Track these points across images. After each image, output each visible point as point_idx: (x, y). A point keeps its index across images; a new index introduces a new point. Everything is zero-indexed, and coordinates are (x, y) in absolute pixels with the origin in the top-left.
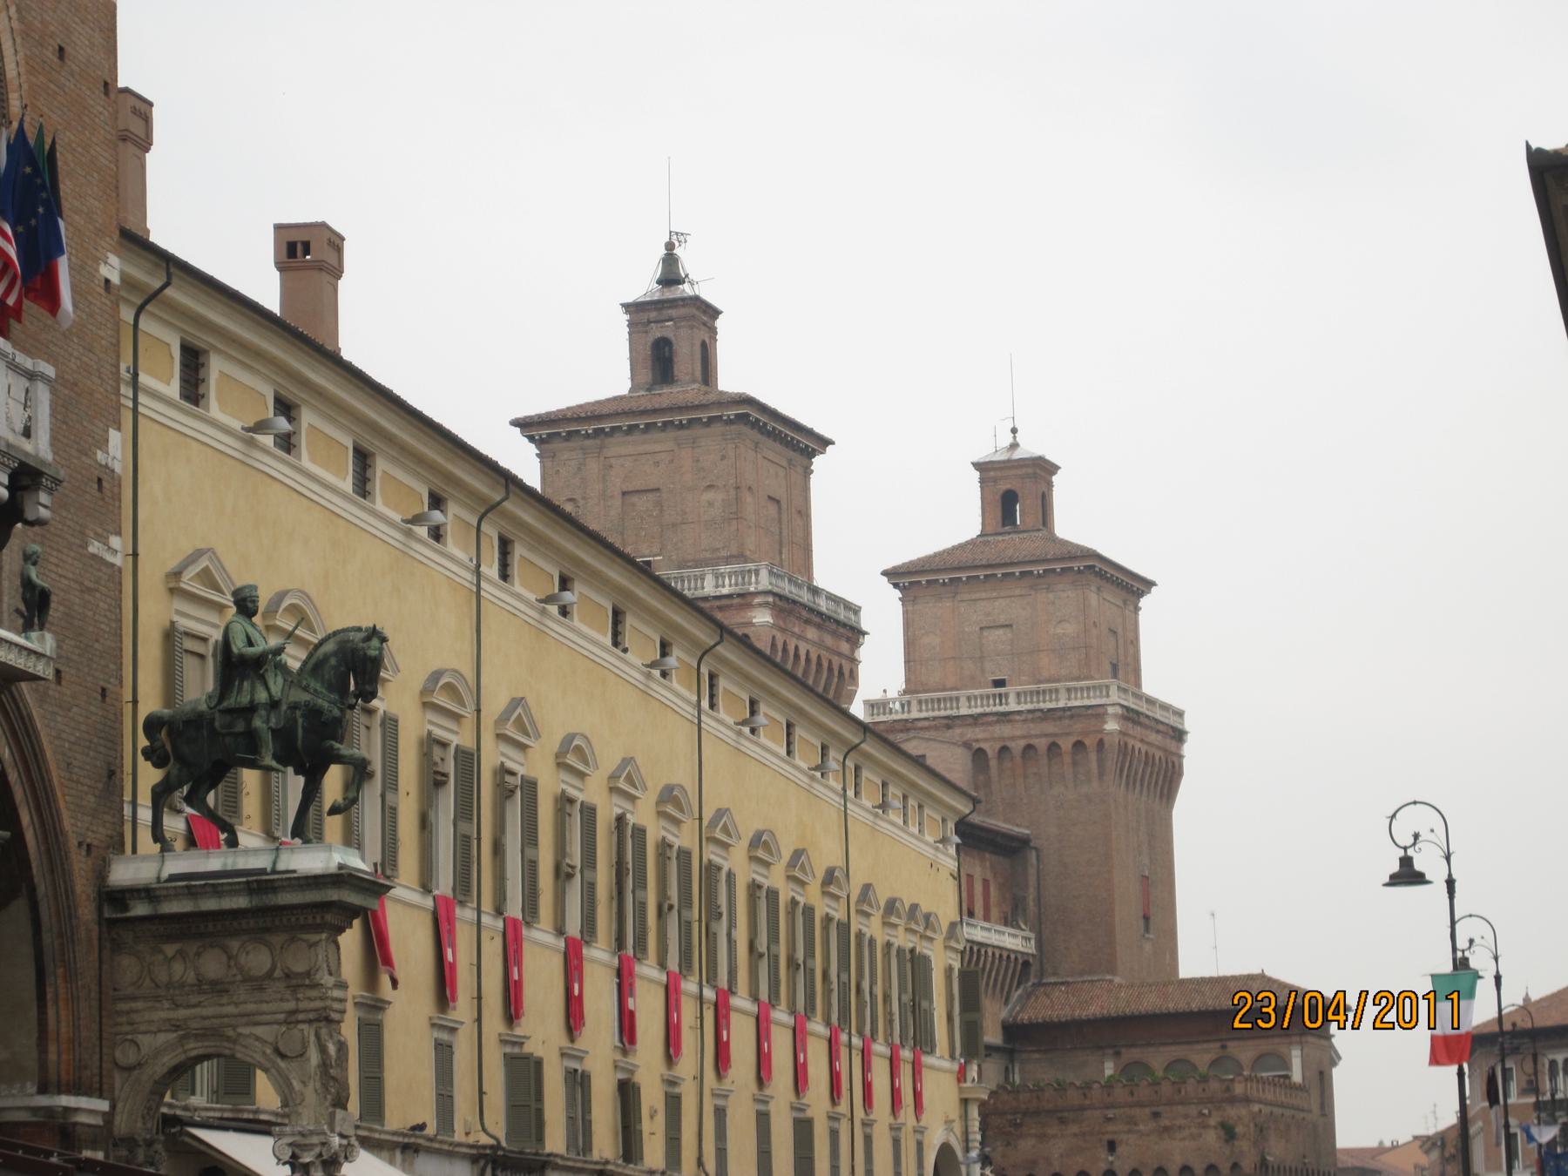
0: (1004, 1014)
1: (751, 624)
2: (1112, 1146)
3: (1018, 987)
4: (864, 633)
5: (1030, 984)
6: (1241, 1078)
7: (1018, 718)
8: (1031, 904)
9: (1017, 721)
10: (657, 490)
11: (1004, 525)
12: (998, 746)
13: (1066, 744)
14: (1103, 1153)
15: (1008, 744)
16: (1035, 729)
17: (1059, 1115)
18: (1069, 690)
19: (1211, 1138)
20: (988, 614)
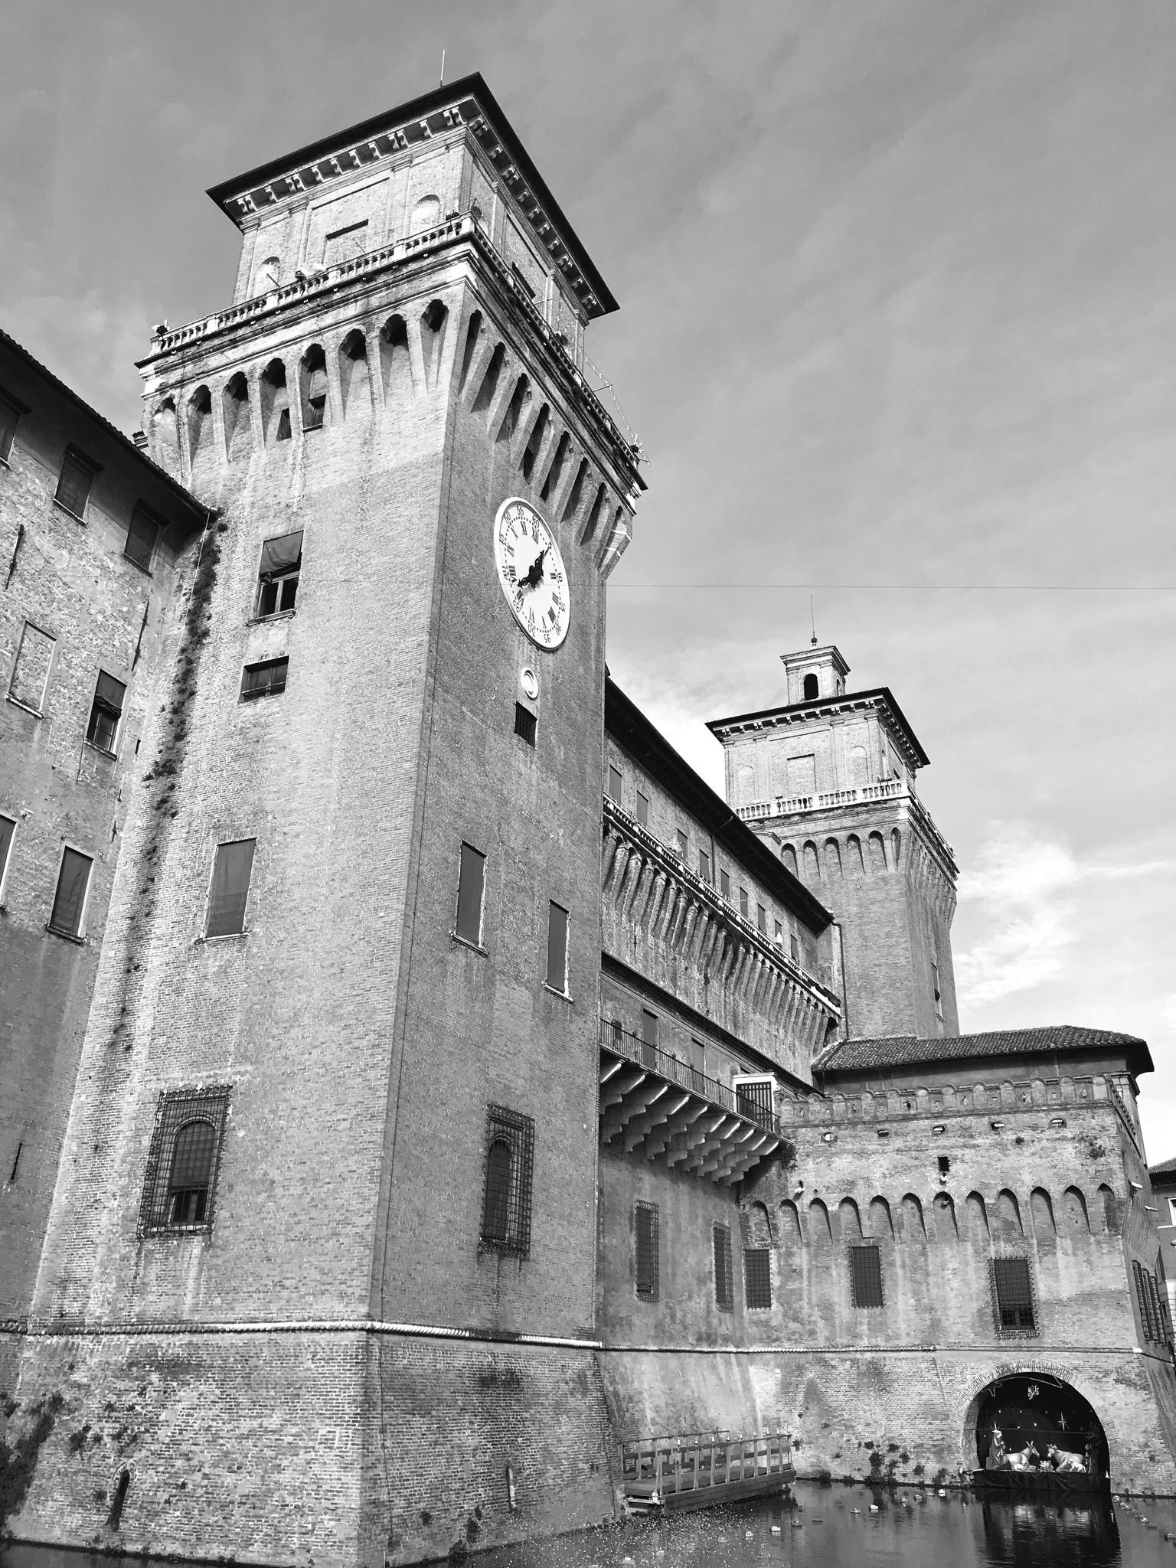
0: (813, 1061)
1: (444, 285)
2: (944, 1164)
3: (826, 1042)
4: (643, 487)
5: (836, 1043)
6: (1102, 1080)
7: (820, 816)
8: (836, 973)
9: (819, 819)
10: (365, 223)
11: (807, 698)
12: (804, 840)
13: (863, 834)
14: (934, 1173)
15: (812, 838)
16: (836, 824)
17: (879, 1127)
18: (865, 790)
19: (1069, 1154)
20: (794, 749)
